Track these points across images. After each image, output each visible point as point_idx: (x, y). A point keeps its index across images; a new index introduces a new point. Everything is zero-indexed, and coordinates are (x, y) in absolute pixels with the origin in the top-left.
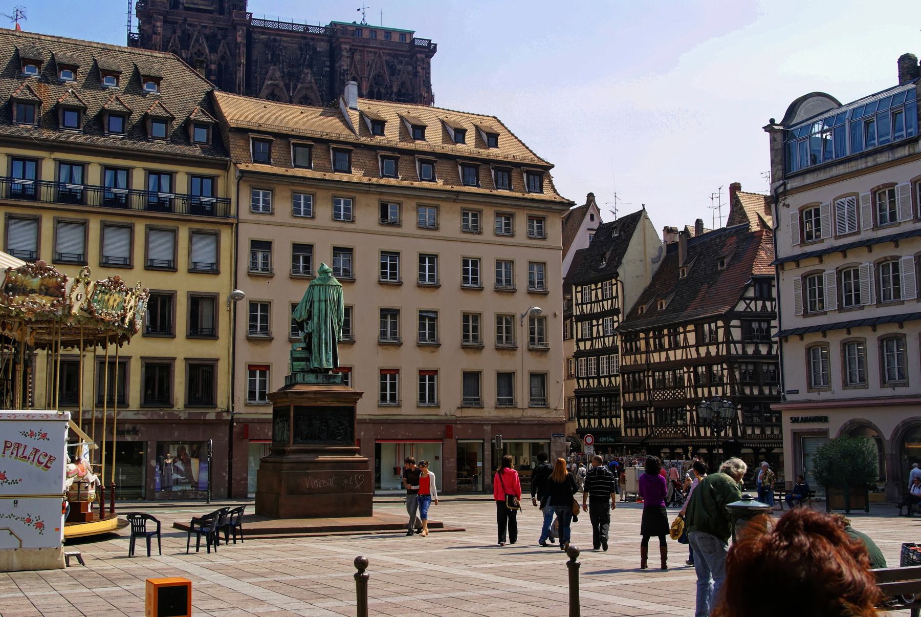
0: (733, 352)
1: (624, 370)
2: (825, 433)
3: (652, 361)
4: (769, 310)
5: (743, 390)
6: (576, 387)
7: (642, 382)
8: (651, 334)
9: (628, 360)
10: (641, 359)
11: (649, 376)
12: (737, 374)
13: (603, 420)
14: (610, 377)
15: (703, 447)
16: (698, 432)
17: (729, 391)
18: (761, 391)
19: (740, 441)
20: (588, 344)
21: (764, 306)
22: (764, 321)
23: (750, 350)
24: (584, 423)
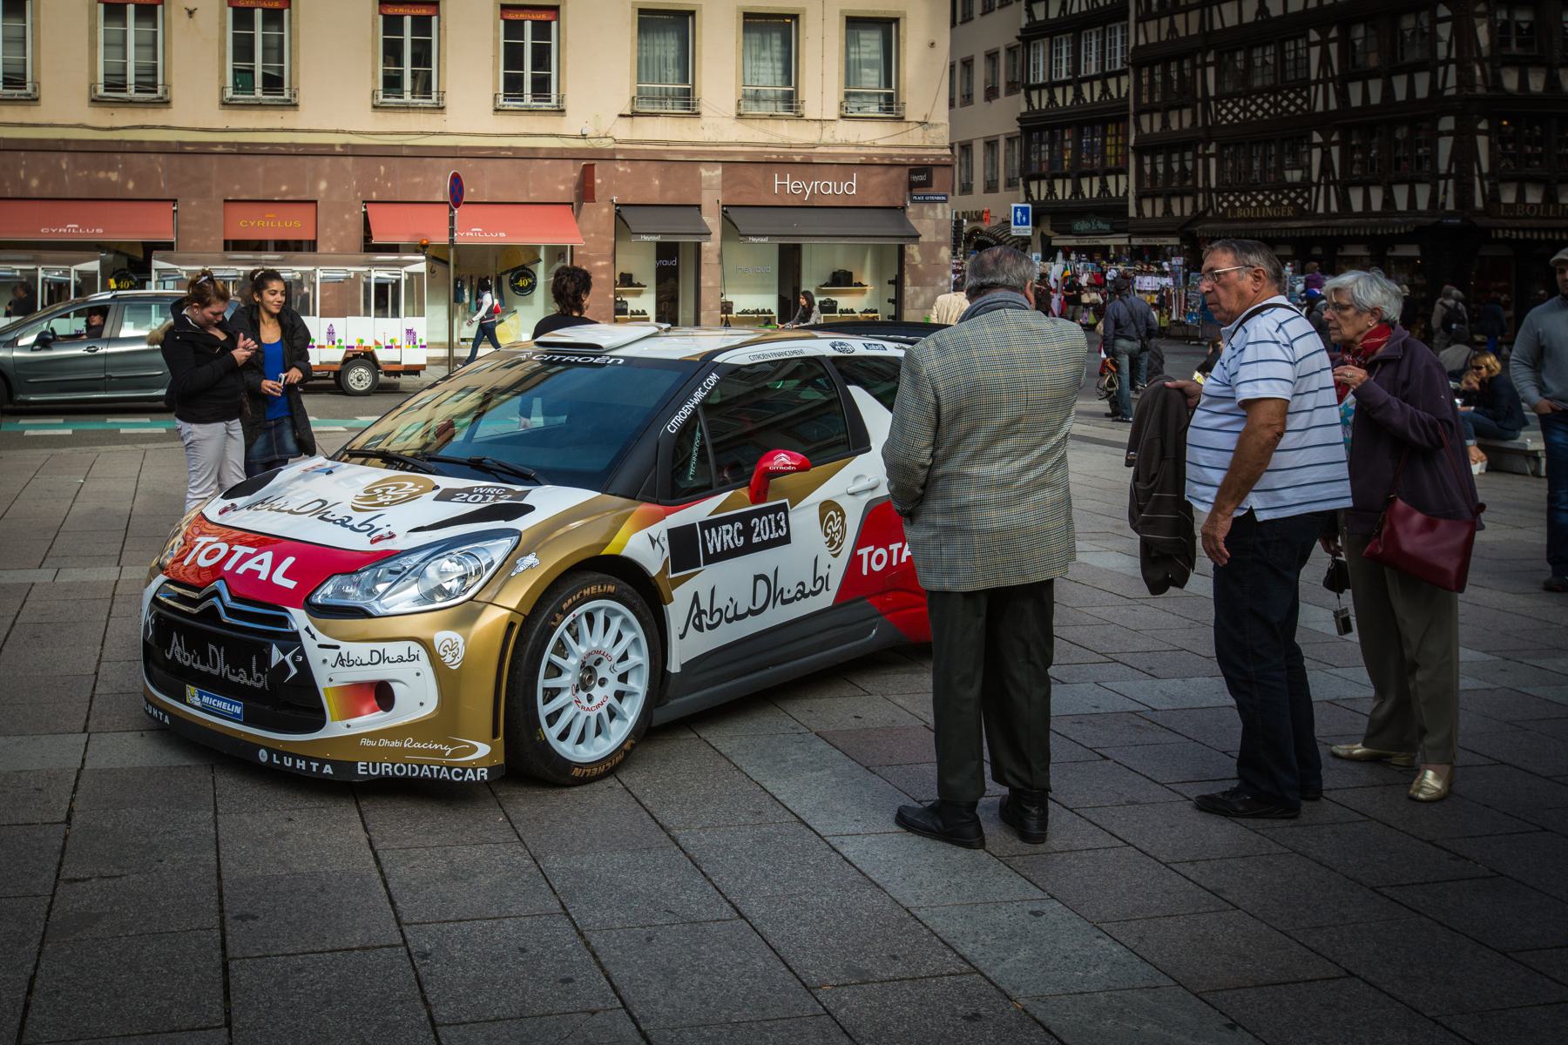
1: (1141, 60)
3: (1217, 25)
5: (1498, 79)
6: (1024, 108)
7: (1187, 86)
9: (1153, 32)
11: (1205, 65)
13: (1085, 183)
14: (1103, 77)
15: (1356, 240)
16: (1344, 202)
17: (1452, 80)
24: (1039, 190)
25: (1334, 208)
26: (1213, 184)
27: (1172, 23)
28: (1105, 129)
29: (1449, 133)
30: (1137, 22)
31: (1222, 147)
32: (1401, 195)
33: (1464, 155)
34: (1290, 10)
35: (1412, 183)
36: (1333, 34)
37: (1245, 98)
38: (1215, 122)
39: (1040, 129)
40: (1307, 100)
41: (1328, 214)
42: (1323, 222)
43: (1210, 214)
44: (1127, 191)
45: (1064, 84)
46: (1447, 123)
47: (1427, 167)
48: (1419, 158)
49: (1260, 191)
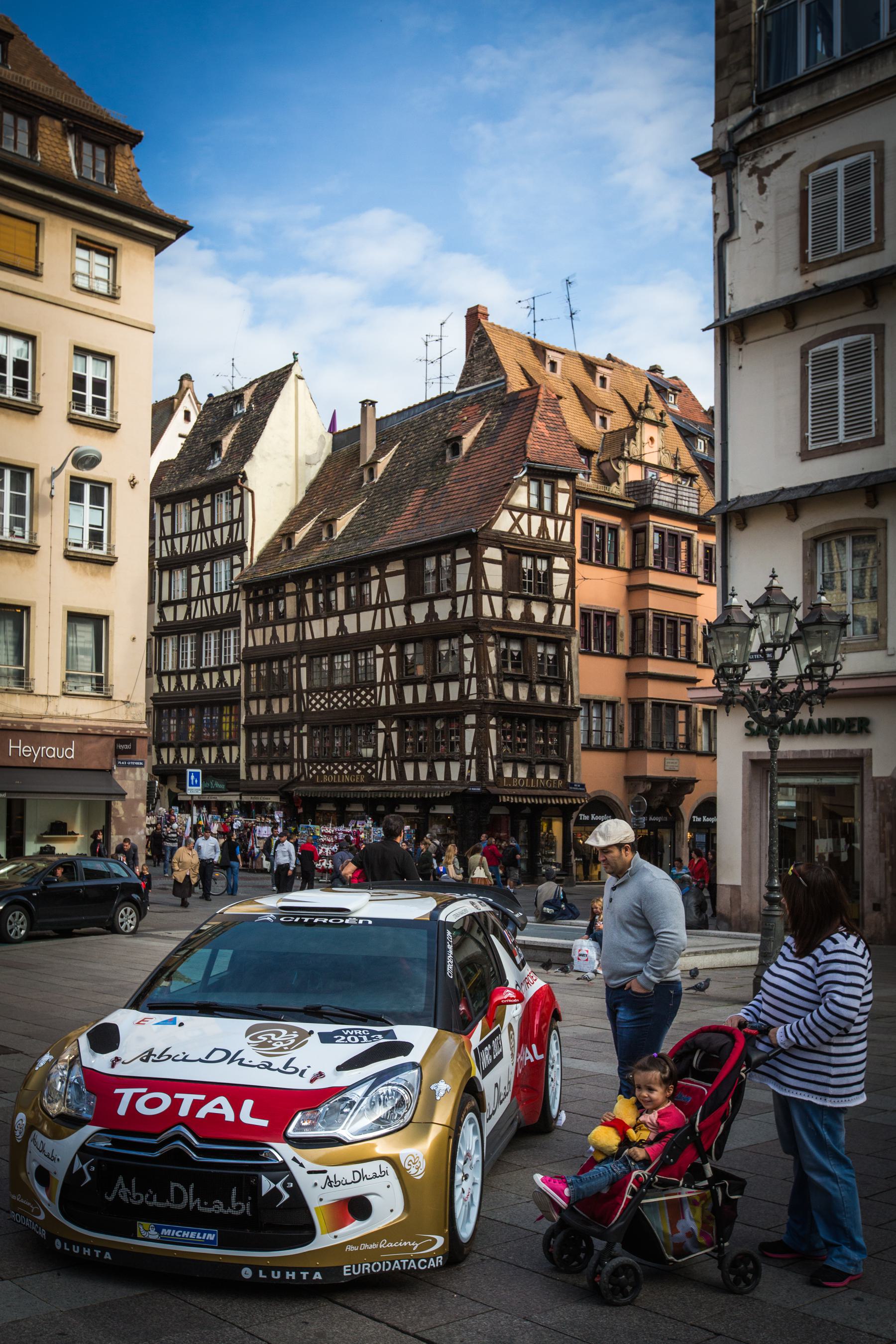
0: (486, 612)
1: (250, 658)
2: (857, 763)
3: (309, 636)
4: (552, 537)
5: (501, 689)
8: (309, 585)
9: (260, 638)
10: (287, 634)
12: (492, 655)
13: (205, 752)
14: (221, 669)
15: (409, 801)
16: (401, 773)
17: (474, 689)
18: (532, 694)
19: (494, 790)
20: (182, 610)
21: (543, 528)
22: (542, 557)
23: (516, 610)
25: (393, 777)
26: (305, 757)
27: (274, 632)
28: (221, 710)
29: (472, 726)
30: (247, 629)
31: (311, 728)
32: (440, 768)
33: (481, 742)
34: (362, 630)
35: (448, 761)
36: (393, 649)
37: (330, 692)
38: (307, 709)
39: (170, 707)
40: (374, 697)
41: (389, 781)
42: (387, 787)
43: (303, 779)
44: (238, 759)
45: (189, 673)
46: (471, 719)
47: (457, 750)
48: (452, 743)
49: (341, 763)
